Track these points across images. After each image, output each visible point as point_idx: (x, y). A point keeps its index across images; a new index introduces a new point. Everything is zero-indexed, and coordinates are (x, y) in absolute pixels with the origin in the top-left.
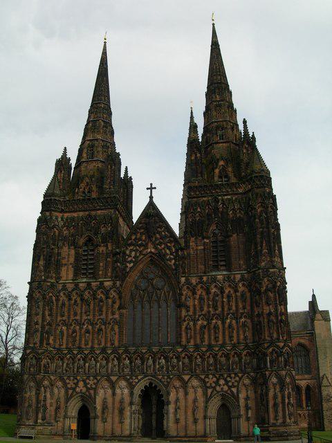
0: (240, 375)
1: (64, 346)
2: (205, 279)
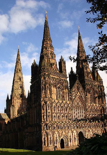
0: (99, 128)
1: (56, 121)
2: (91, 105)
